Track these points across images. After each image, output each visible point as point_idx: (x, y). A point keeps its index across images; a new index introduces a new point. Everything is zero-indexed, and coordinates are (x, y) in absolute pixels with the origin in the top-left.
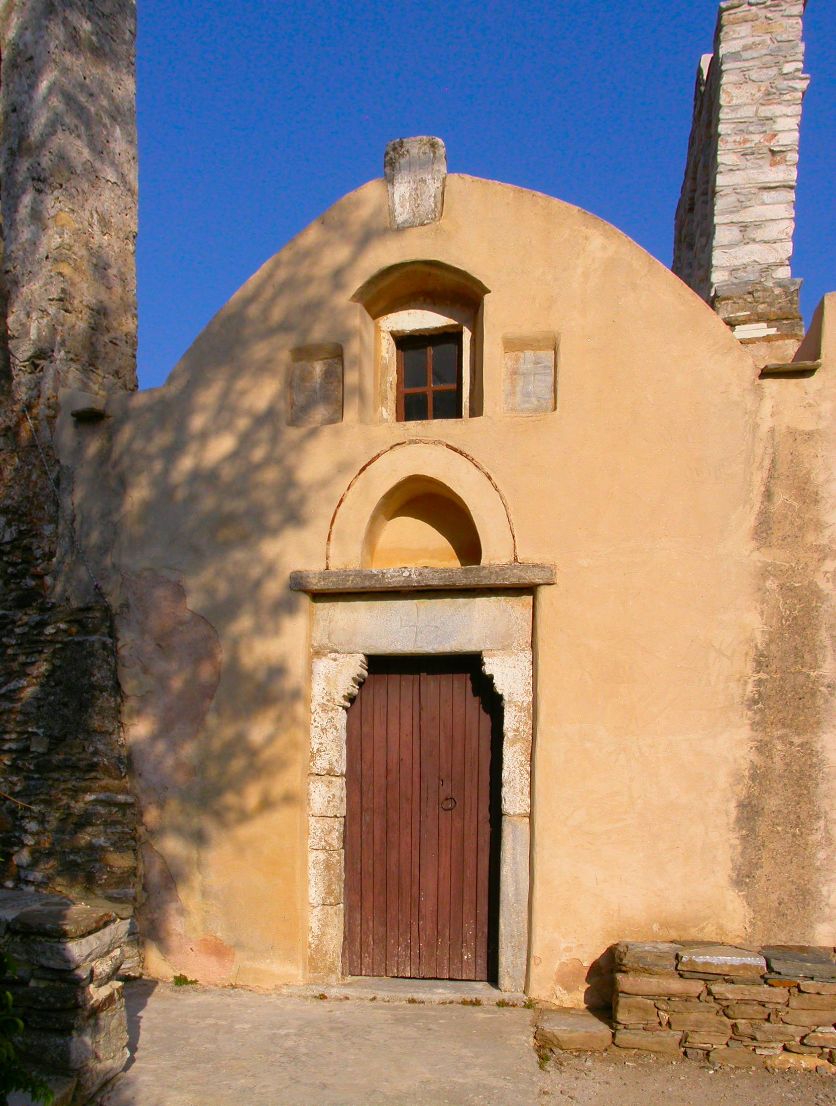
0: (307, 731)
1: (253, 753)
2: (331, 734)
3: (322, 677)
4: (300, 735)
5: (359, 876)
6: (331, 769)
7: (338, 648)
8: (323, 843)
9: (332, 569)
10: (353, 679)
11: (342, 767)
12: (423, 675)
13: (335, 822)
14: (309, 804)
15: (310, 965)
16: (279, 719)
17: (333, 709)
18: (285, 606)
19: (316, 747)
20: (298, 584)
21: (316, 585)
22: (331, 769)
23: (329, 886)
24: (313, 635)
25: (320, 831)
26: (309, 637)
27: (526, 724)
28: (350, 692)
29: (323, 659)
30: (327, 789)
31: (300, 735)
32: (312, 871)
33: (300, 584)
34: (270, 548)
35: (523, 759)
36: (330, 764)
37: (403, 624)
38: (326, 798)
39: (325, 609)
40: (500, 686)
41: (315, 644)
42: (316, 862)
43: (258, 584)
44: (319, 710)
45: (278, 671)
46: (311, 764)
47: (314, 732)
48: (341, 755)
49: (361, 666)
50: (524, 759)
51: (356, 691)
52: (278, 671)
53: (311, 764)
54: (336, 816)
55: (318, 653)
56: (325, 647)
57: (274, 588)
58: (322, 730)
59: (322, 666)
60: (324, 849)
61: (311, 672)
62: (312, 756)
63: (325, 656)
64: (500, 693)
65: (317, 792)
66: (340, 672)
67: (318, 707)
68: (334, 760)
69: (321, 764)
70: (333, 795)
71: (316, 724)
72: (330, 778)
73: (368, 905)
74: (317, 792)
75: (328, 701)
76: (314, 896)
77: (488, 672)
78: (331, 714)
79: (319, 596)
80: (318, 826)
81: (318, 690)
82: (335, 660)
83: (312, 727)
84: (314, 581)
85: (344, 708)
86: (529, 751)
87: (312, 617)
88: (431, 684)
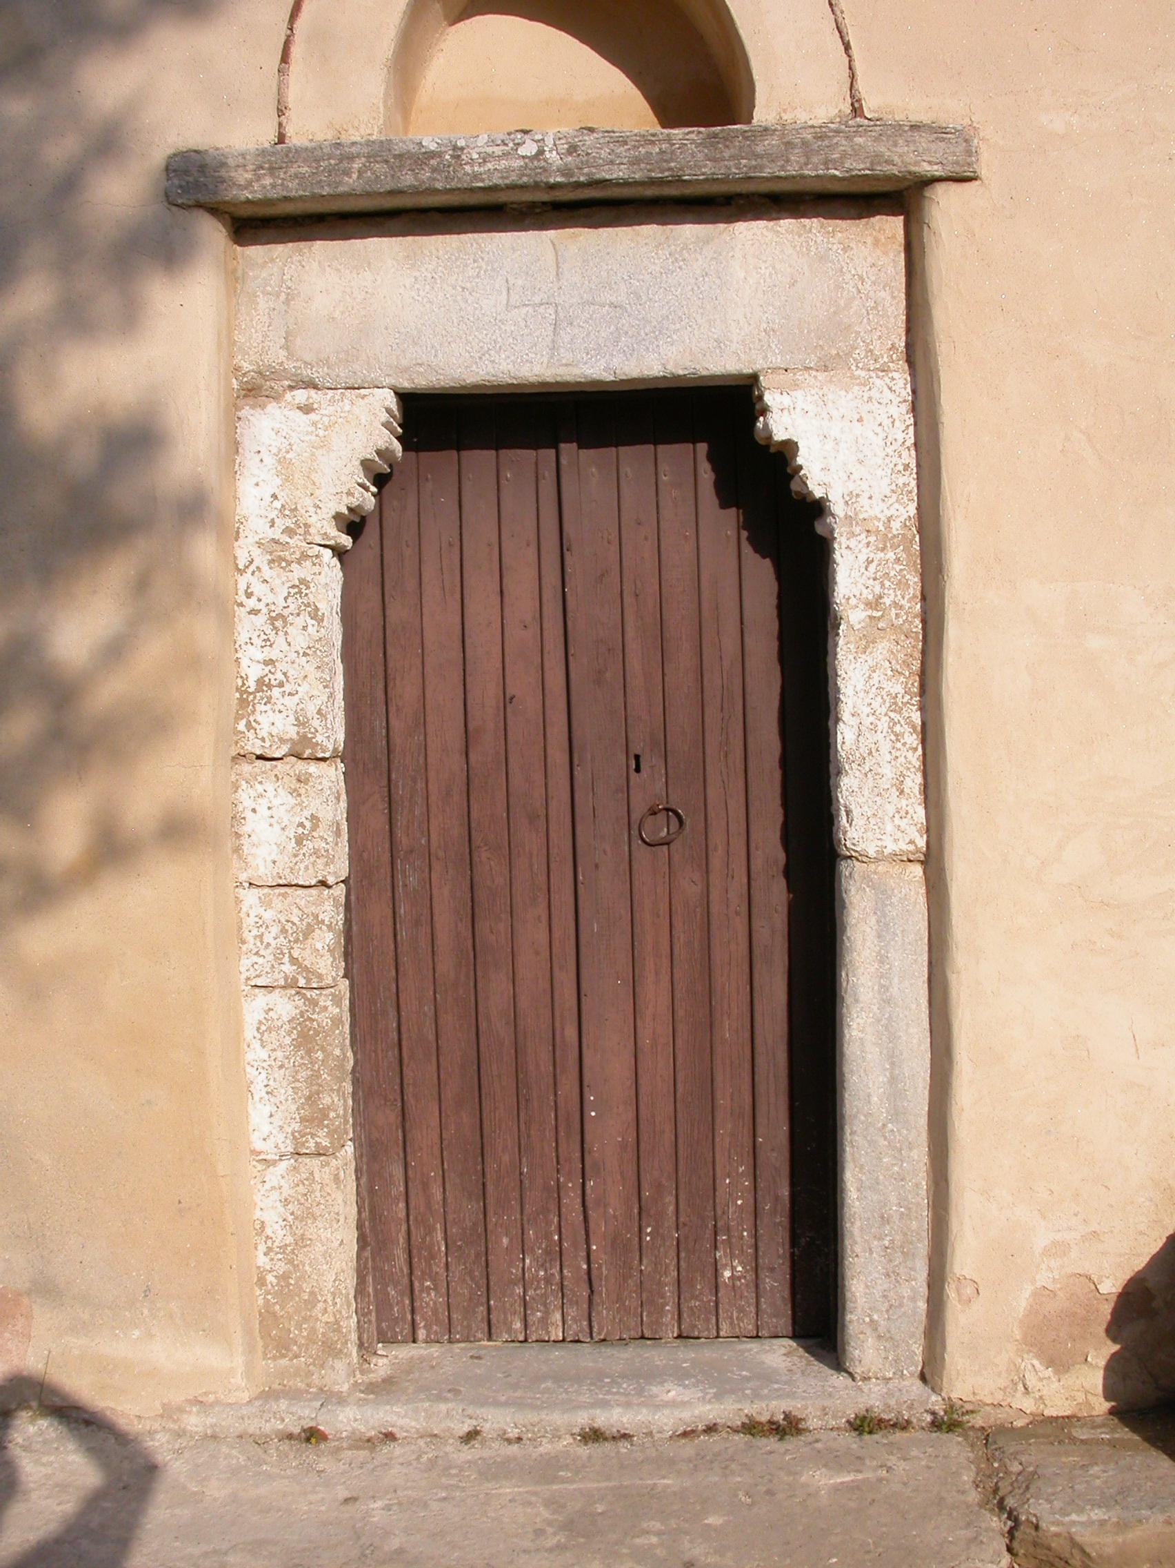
0: (227, 622)
1: (60, 693)
2: (300, 634)
3: (269, 461)
4: (204, 632)
5: (392, 1054)
6: (304, 740)
7: (316, 374)
8: (288, 968)
9: (296, 138)
10: (366, 464)
11: (333, 734)
12: (568, 450)
13: (319, 902)
14: (237, 850)
15: (265, 1334)
16: (142, 585)
17: (304, 556)
18: (153, 247)
19: (254, 672)
20: (193, 187)
21: (250, 187)
22: (304, 740)
23: (311, 1099)
24: (240, 338)
25: (275, 930)
26: (227, 342)
27: (902, 584)
28: (354, 502)
29: (272, 407)
30: (292, 801)
31: (204, 632)
32: (256, 1053)
33: (197, 186)
34: (108, 82)
35: (899, 689)
36: (299, 723)
37: (515, 298)
38: (287, 829)
39: (273, 261)
40: (819, 472)
41: (246, 366)
42: (266, 1028)
43: (69, 185)
44: (261, 560)
45: (134, 439)
46: (241, 726)
47: (247, 628)
48: (331, 696)
49: (386, 425)
50: (902, 687)
51: (370, 502)
52: (134, 439)
53: (241, 726)
54: (323, 884)
55: (254, 391)
56: (276, 374)
57: (120, 193)
58: (272, 620)
59: (268, 426)
60: (291, 984)
61: (235, 446)
62: (243, 703)
63: (277, 398)
64: (818, 493)
65: (263, 811)
66: (324, 444)
67: (256, 552)
68: (311, 709)
69: (273, 724)
70: (314, 818)
71: (251, 603)
72: (301, 766)
73: (425, 1136)
74: (263, 811)
75: (289, 531)
76: (266, 1129)
77: (779, 435)
78: (298, 572)
79: (255, 225)
80: (268, 915)
81: (255, 499)
82: (307, 409)
83: (241, 612)
84: (243, 176)
85: (339, 552)
86: (916, 665)
87: (233, 280)
88: (594, 476)
